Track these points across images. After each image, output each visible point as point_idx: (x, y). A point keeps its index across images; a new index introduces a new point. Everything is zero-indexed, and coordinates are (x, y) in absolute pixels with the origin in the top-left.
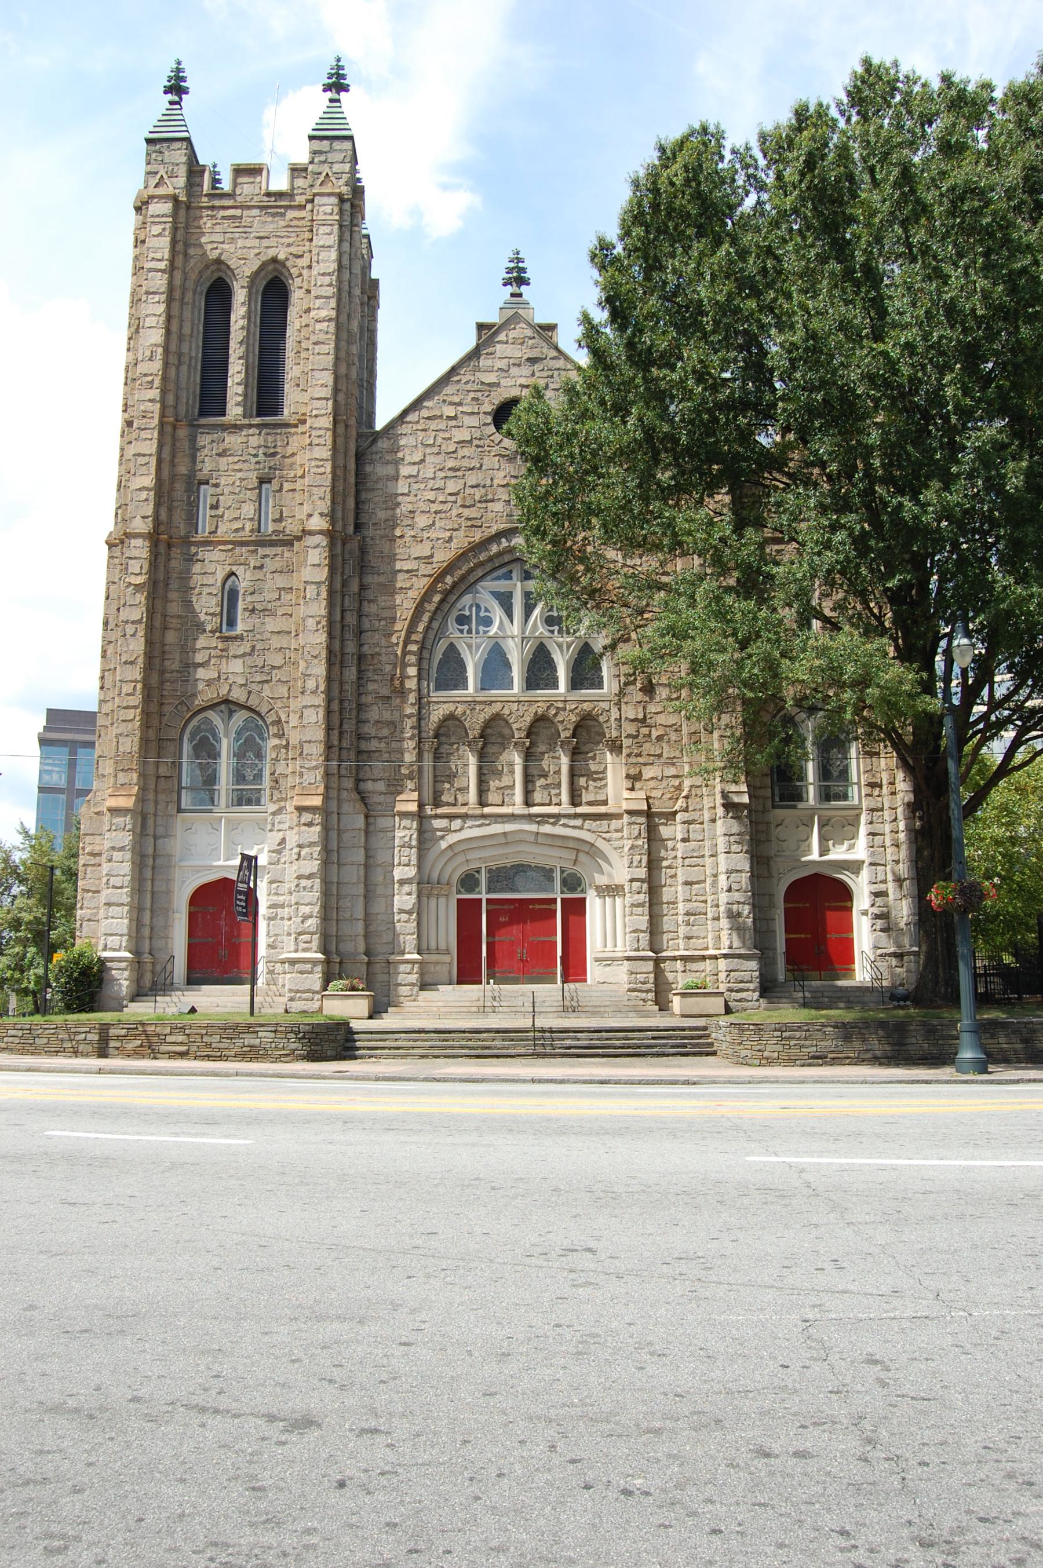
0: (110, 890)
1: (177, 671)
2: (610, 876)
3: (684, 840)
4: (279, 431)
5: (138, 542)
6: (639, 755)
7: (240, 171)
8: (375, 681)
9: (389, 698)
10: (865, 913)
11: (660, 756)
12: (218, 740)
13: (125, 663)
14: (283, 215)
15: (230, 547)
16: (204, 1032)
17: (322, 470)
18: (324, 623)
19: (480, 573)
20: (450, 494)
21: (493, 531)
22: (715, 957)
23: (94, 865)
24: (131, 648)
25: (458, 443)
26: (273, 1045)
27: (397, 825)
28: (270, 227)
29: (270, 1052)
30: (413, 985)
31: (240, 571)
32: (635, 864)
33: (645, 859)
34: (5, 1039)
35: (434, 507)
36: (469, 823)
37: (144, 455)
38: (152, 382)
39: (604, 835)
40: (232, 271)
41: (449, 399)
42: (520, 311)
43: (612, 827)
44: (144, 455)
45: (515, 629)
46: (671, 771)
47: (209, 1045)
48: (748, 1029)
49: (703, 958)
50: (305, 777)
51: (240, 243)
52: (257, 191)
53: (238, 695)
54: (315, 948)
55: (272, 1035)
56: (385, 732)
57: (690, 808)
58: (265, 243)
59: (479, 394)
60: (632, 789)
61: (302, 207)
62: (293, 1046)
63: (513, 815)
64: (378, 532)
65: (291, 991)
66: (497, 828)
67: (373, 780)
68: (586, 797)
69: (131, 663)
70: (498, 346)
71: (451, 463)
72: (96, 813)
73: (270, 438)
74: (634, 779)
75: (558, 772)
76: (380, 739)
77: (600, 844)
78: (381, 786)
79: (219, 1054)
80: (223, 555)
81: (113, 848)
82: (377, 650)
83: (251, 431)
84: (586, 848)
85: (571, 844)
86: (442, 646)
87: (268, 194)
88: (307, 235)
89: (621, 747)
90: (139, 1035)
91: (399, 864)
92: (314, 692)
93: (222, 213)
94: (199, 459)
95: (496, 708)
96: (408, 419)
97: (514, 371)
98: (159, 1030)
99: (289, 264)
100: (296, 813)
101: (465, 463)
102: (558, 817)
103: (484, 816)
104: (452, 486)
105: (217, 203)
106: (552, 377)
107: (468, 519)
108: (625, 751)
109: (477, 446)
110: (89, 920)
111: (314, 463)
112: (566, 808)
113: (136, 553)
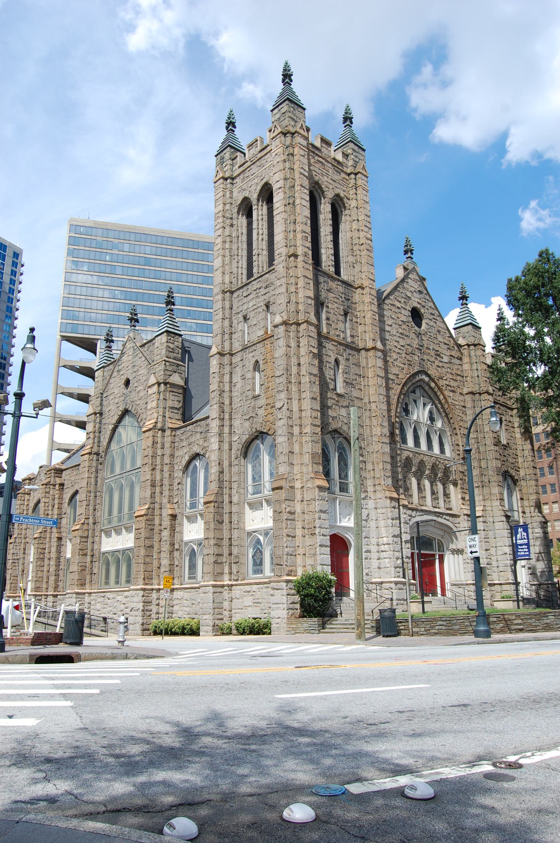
0: (322, 537)
2: (456, 544)
3: (484, 530)
4: (349, 288)
5: (312, 328)
6: (464, 489)
7: (323, 140)
10: (524, 567)
12: (329, 453)
13: (313, 398)
14: (340, 174)
15: (336, 344)
17: (375, 317)
18: (385, 399)
20: (402, 346)
22: (501, 584)
23: (291, 520)
24: (314, 390)
25: (402, 321)
26: (555, 622)
27: (401, 513)
31: (340, 358)
34: (437, 627)
36: (418, 514)
37: (308, 278)
38: (307, 237)
39: (456, 525)
40: (323, 192)
41: (398, 298)
44: (308, 278)
47: (531, 624)
49: (495, 584)
50: (386, 481)
54: (402, 576)
55: (553, 617)
58: (336, 185)
60: (463, 504)
61: (346, 173)
63: (430, 512)
65: (397, 599)
69: (315, 399)
71: (401, 331)
72: (290, 487)
73: (347, 291)
75: (437, 492)
80: (334, 348)
81: (321, 511)
83: (339, 283)
84: (449, 530)
85: (445, 528)
87: (334, 159)
88: (353, 191)
89: (457, 483)
92: (385, 436)
93: (317, 158)
94: (320, 289)
96: (386, 302)
97: (415, 293)
98: (510, 617)
99: (345, 200)
100: (388, 501)
101: (404, 332)
102: (443, 514)
103: (422, 511)
104: (402, 342)
105: (316, 152)
107: (408, 360)
108: (459, 487)
109: (408, 326)
110: (291, 555)
111: (373, 313)
113: (312, 334)
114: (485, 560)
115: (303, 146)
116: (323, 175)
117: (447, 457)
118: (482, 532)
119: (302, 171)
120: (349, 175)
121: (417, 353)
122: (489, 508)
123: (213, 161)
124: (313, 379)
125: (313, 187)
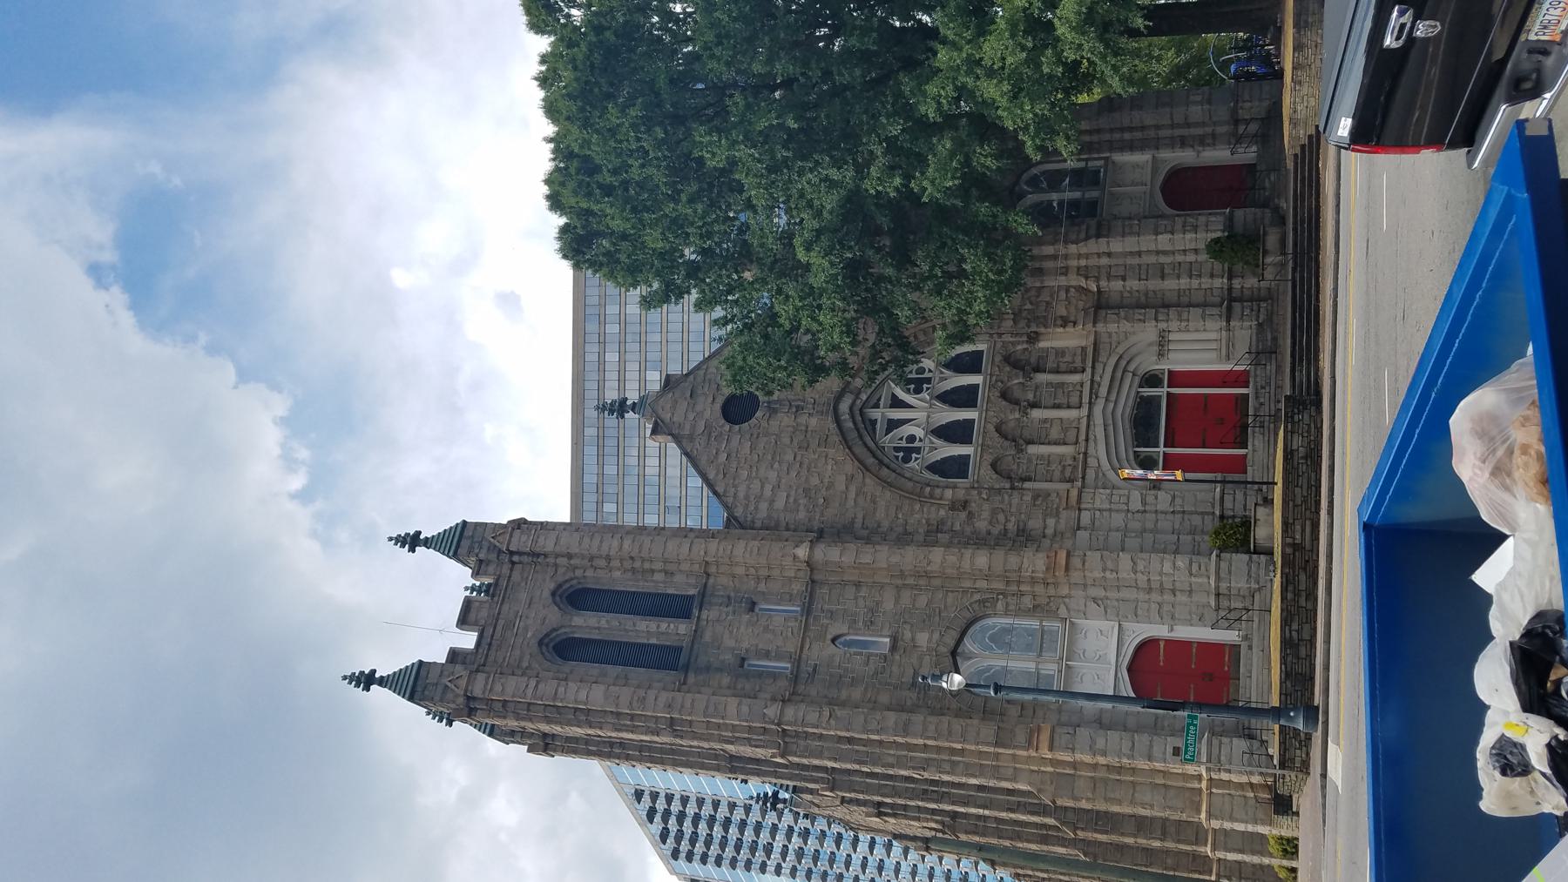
1: (918, 693)
8: (952, 524)
9: (970, 513)
11: (1047, 303)
12: (989, 668)
16: (1291, 503)
19: (868, 439)
21: (833, 426)
28: (523, 596)
29: (1312, 438)
30: (1245, 494)
32: (1142, 317)
33: (1137, 311)
35: (804, 472)
36: (1091, 451)
37: (707, 707)
42: (648, 402)
43: (1108, 340)
45: (920, 415)
46: (1063, 295)
47: (1305, 501)
48: (1298, 57)
51: (530, 622)
52: (487, 605)
53: (950, 641)
56: (1001, 517)
57: (1096, 275)
59: (713, 434)
60: (1075, 323)
62: (1306, 417)
63: (1089, 416)
64: (817, 518)
66: (1099, 431)
67: (1045, 528)
68: (1078, 364)
70: (675, 419)
74: (1065, 322)
76: (1007, 521)
77: (1120, 350)
78: (1051, 522)
79: (1313, 488)
82: (924, 521)
86: (928, 475)
89: (1036, 333)
90: (1294, 572)
91: (1127, 504)
95: (991, 428)
97: (699, 408)
99: (560, 579)
103: (1087, 440)
106: (710, 380)
108: (1042, 330)
112: (1087, 376)
114: (1182, 281)
115: (487, 683)
116: (526, 629)
117: (989, 349)
118: (1128, 283)
119: (530, 691)
120: (513, 563)
121: (803, 419)
122: (1083, 262)
123: (511, 745)
124: (874, 725)
125: (547, 645)
